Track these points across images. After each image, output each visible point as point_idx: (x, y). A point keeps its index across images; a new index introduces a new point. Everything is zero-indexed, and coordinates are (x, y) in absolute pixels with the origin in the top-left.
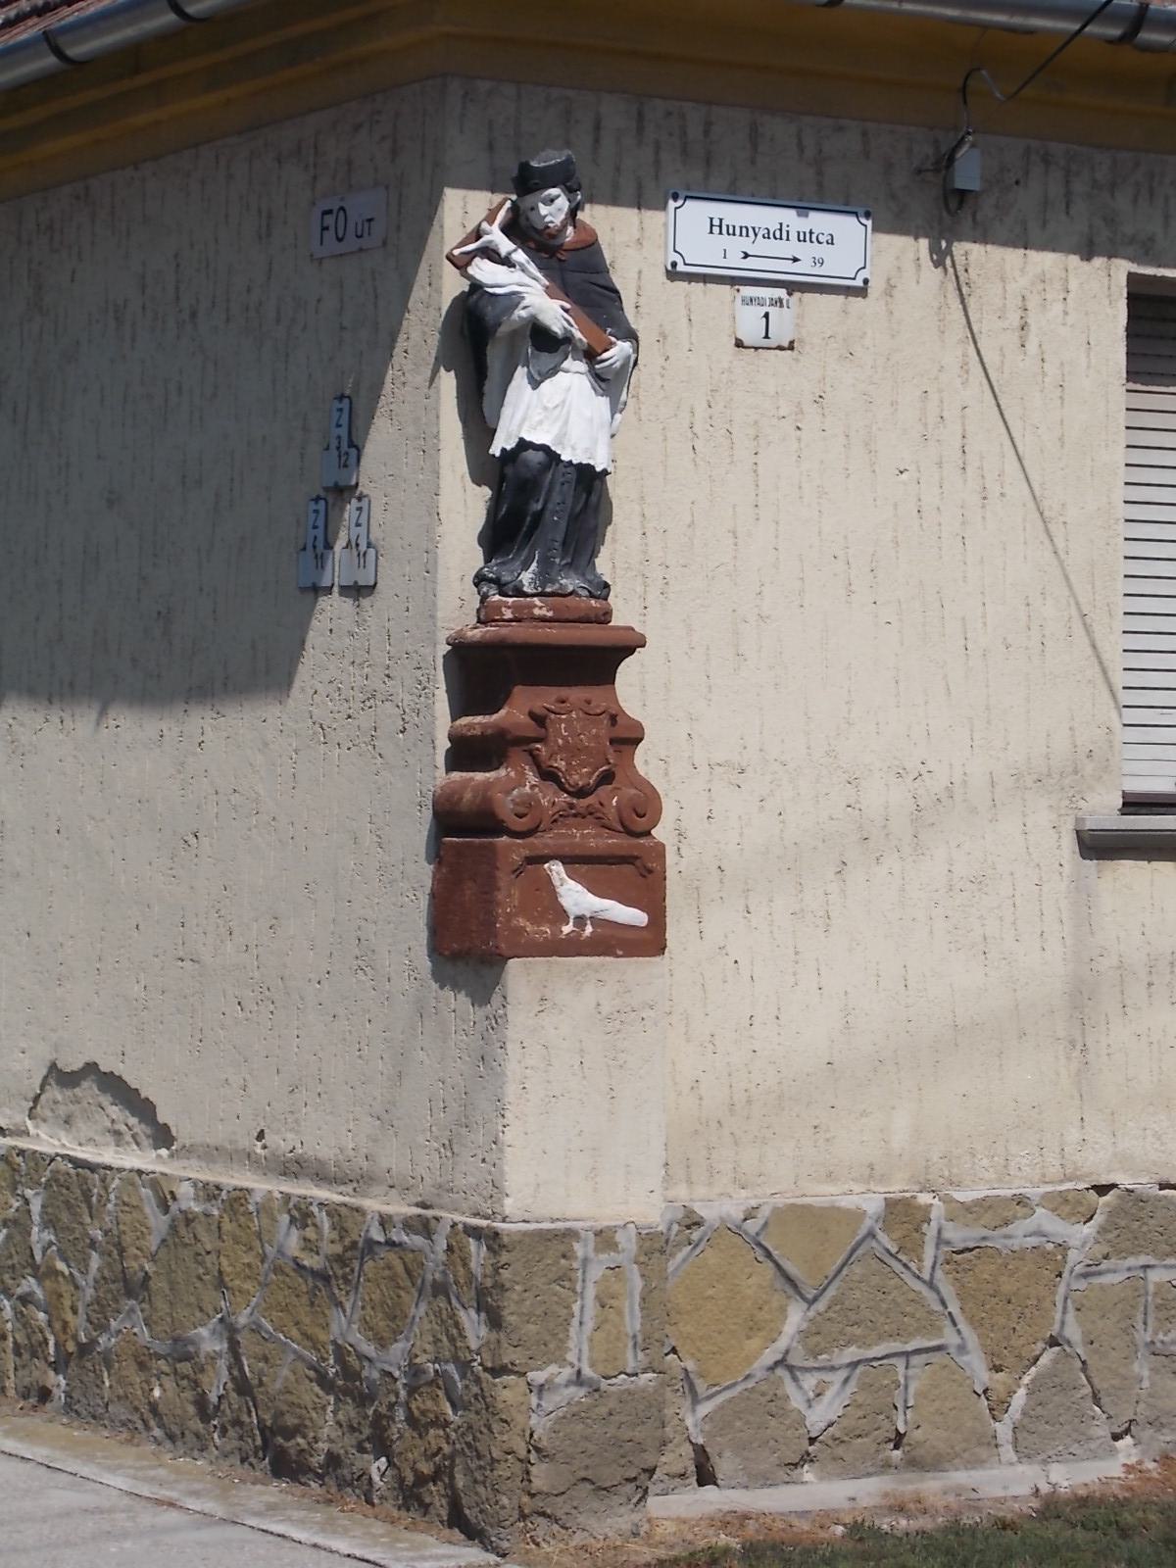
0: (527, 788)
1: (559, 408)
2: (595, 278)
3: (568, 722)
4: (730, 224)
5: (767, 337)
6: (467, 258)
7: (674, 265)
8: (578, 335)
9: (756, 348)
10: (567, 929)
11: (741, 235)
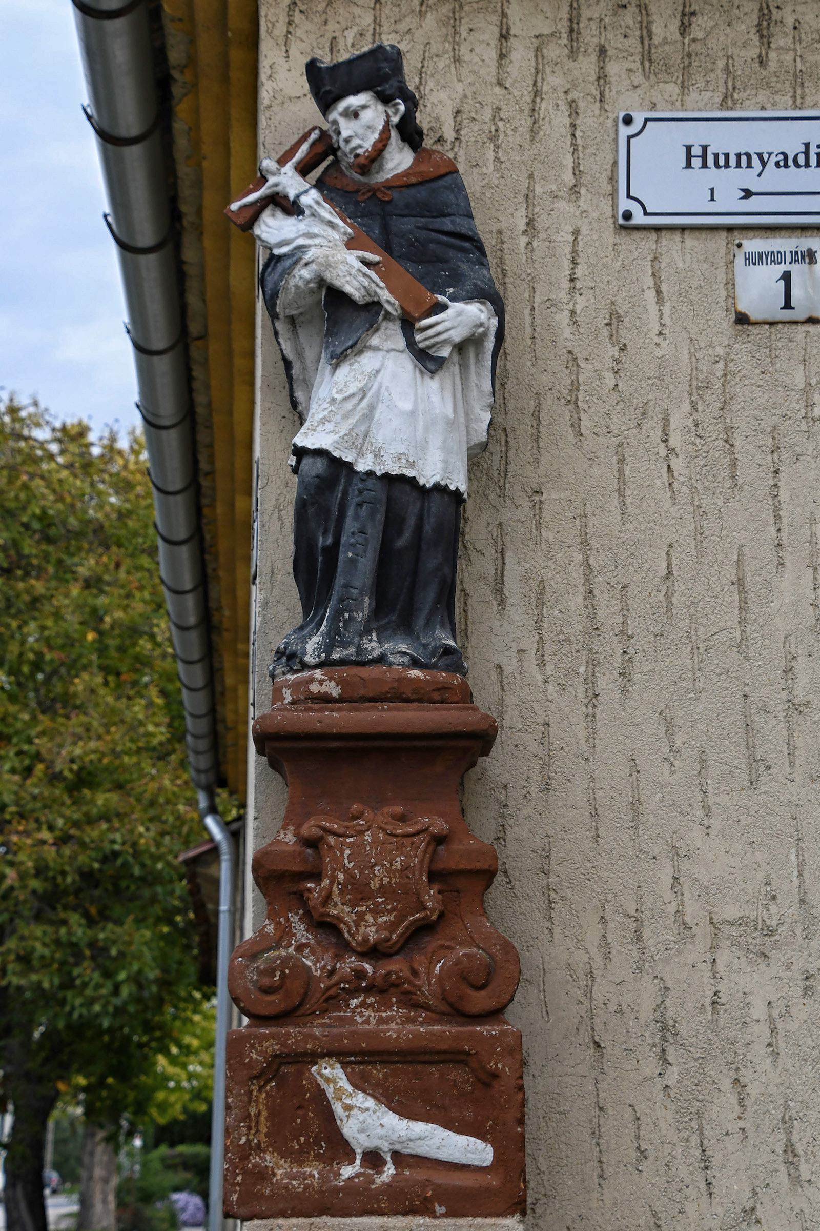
0: (291, 950)
1: (355, 401)
2: (447, 224)
3: (358, 848)
4: (721, 151)
5: (788, 305)
6: (248, 214)
7: (628, 215)
8: (385, 295)
9: (772, 324)
10: (347, 1171)
11: (739, 165)
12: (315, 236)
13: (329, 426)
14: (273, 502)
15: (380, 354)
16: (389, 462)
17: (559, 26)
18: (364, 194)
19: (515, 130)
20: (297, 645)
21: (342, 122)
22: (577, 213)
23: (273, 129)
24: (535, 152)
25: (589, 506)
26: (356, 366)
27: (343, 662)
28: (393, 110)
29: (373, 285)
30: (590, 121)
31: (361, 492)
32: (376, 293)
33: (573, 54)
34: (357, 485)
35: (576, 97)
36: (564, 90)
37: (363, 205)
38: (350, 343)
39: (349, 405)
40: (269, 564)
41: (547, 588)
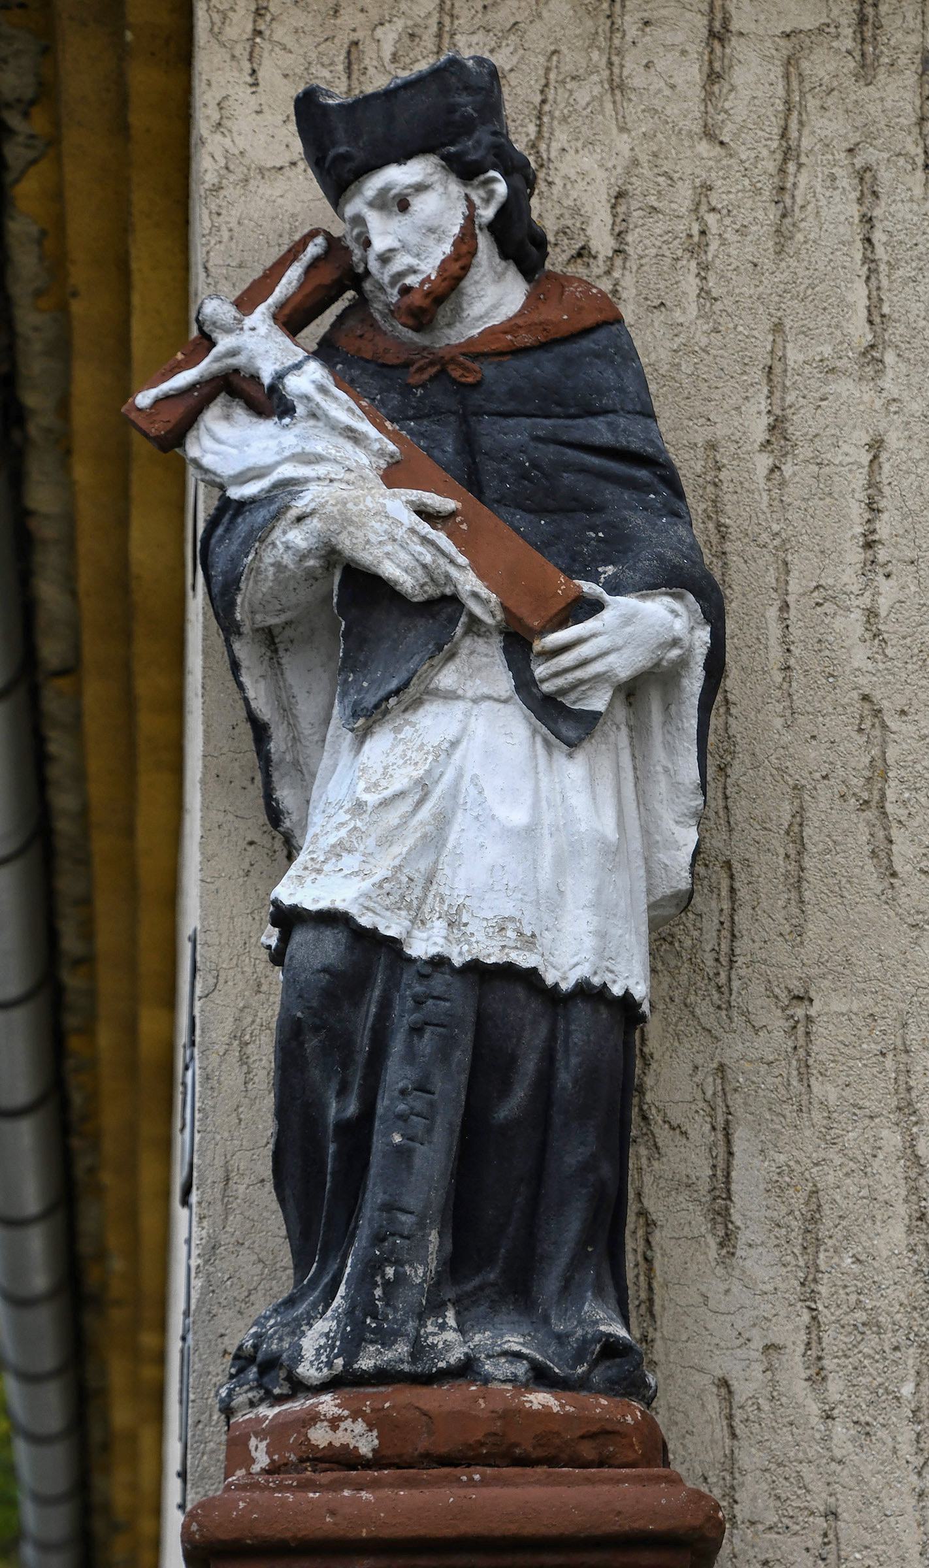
8: (468, 582)
12: (317, 459)
13: (350, 862)
14: (229, 1026)
15: (459, 707)
16: (480, 936)
17: (836, 12)
18: (421, 370)
19: (742, 231)
20: (281, 1339)
21: (374, 220)
22: (878, 404)
23: (226, 235)
24: (786, 276)
25: (914, 1029)
26: (408, 731)
27: (383, 1376)
28: (482, 193)
29: (442, 561)
30: (903, 210)
31: (419, 1002)
32: (448, 577)
33: (866, 70)
34: (412, 987)
35: (872, 160)
36: (847, 145)
37: (420, 392)
38: (394, 684)
39: (392, 817)
40: (220, 1161)
41: (826, 1207)
